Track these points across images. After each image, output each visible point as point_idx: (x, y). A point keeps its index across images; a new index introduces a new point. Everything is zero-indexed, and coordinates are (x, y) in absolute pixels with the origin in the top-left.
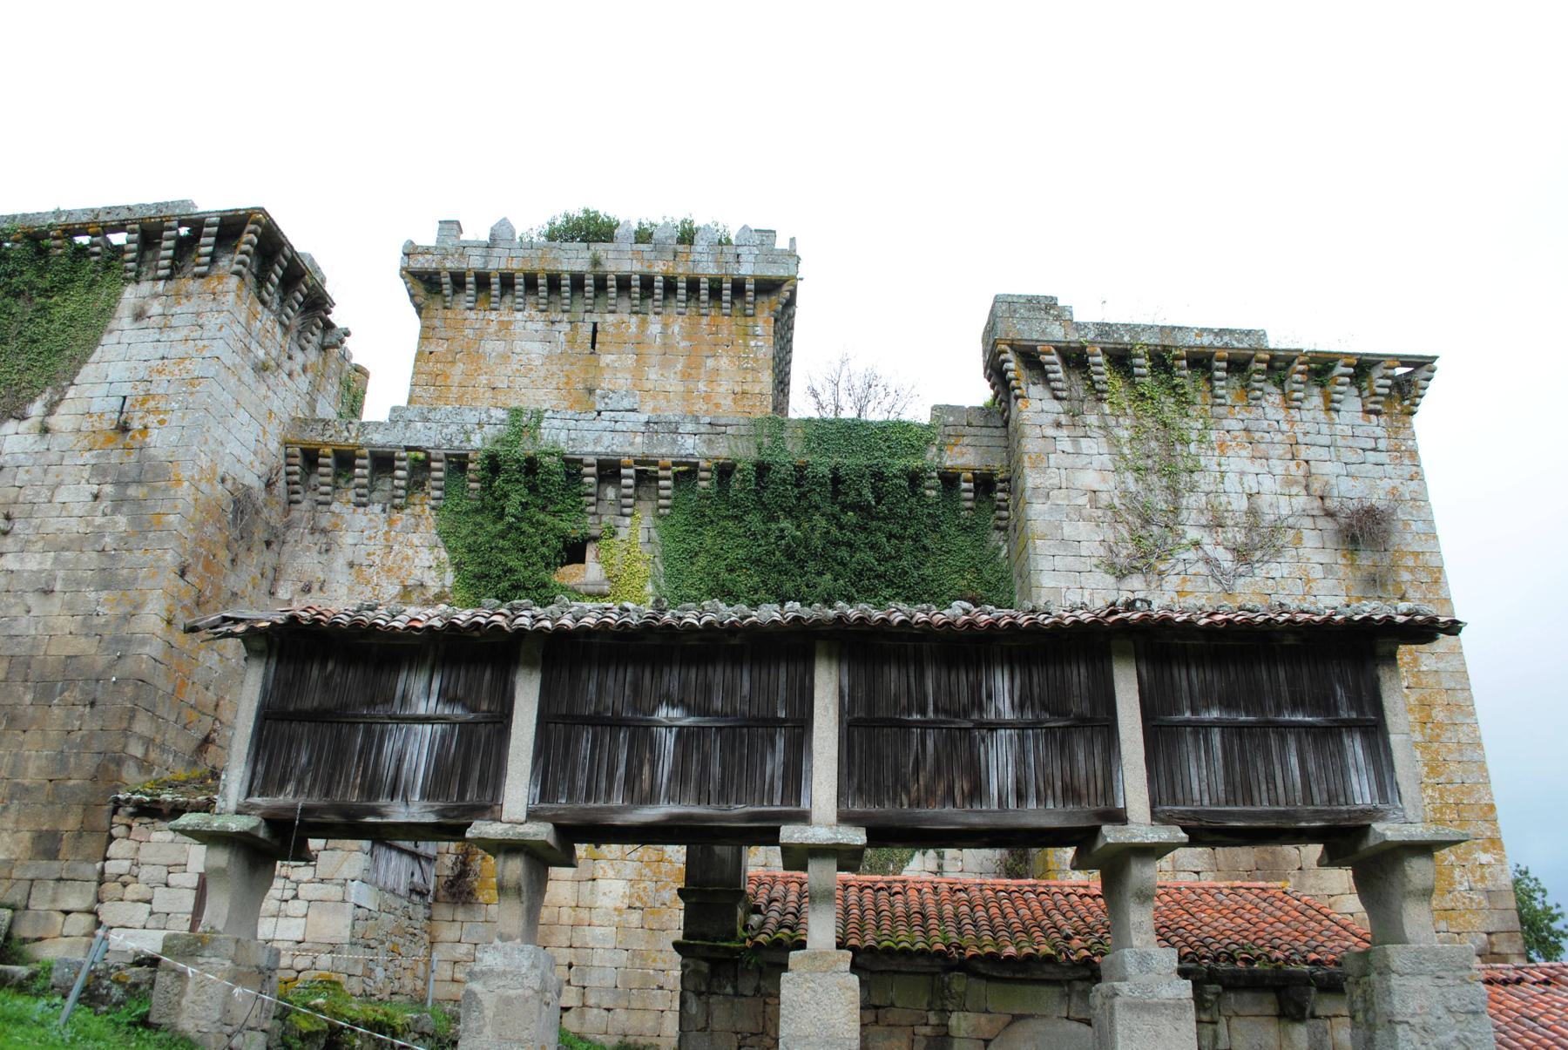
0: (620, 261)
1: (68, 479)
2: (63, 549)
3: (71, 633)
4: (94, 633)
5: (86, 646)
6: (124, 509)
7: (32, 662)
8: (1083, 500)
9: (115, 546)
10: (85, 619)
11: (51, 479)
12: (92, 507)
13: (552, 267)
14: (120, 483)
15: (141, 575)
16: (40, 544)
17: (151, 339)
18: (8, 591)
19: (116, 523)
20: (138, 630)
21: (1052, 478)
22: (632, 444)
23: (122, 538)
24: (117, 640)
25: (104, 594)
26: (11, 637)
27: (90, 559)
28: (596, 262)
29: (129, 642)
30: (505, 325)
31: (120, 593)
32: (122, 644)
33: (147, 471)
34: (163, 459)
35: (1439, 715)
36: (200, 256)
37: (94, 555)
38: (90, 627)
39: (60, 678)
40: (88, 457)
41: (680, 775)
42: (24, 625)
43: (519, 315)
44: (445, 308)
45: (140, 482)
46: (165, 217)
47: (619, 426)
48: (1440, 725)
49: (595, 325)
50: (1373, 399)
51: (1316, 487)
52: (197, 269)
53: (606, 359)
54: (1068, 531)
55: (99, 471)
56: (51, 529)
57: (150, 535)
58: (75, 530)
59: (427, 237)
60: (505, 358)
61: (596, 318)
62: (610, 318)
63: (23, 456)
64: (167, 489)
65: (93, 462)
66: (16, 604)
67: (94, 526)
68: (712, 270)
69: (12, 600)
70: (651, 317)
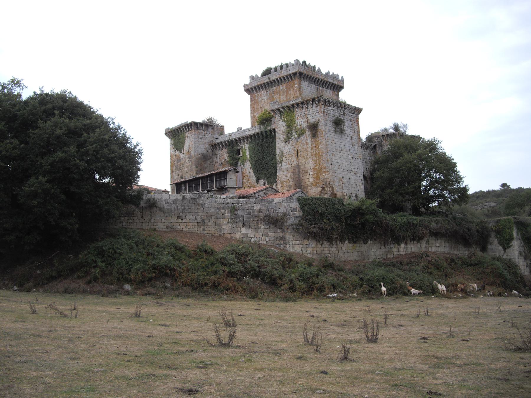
0: (274, 76)
13: (263, 82)
21: (279, 129)
28: (269, 79)
30: (261, 95)
35: (321, 154)
40: (187, 156)
41: (195, 189)
43: (262, 92)
48: (321, 156)
51: (309, 121)
53: (275, 96)
59: (248, 82)
60: (261, 101)
61: (272, 89)
62: (275, 88)
68: (286, 74)
70: (281, 86)
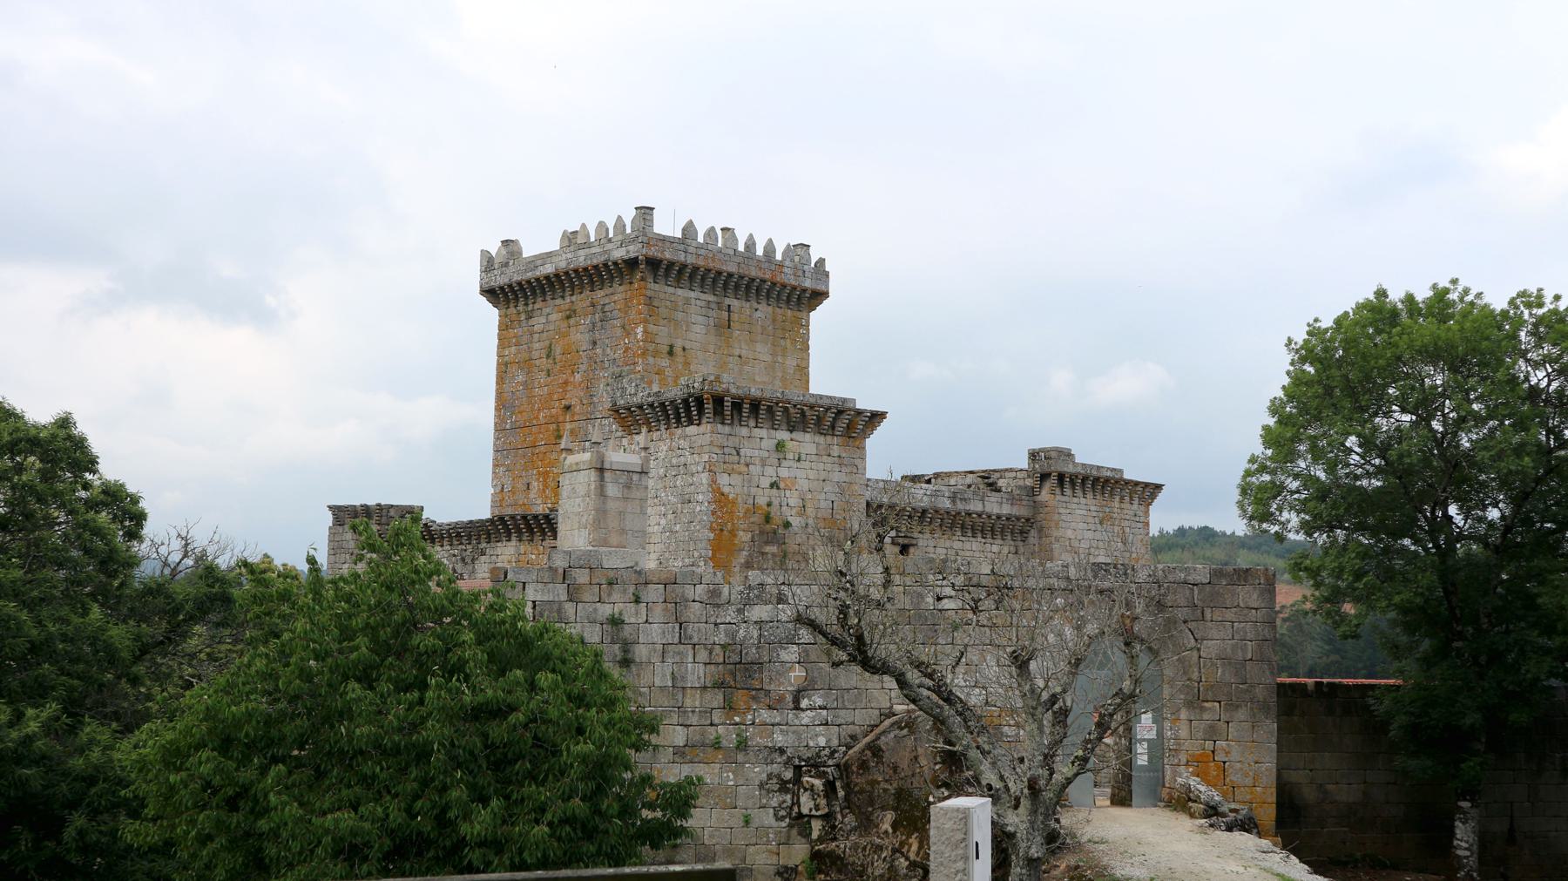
30: (687, 301)
49: (729, 306)
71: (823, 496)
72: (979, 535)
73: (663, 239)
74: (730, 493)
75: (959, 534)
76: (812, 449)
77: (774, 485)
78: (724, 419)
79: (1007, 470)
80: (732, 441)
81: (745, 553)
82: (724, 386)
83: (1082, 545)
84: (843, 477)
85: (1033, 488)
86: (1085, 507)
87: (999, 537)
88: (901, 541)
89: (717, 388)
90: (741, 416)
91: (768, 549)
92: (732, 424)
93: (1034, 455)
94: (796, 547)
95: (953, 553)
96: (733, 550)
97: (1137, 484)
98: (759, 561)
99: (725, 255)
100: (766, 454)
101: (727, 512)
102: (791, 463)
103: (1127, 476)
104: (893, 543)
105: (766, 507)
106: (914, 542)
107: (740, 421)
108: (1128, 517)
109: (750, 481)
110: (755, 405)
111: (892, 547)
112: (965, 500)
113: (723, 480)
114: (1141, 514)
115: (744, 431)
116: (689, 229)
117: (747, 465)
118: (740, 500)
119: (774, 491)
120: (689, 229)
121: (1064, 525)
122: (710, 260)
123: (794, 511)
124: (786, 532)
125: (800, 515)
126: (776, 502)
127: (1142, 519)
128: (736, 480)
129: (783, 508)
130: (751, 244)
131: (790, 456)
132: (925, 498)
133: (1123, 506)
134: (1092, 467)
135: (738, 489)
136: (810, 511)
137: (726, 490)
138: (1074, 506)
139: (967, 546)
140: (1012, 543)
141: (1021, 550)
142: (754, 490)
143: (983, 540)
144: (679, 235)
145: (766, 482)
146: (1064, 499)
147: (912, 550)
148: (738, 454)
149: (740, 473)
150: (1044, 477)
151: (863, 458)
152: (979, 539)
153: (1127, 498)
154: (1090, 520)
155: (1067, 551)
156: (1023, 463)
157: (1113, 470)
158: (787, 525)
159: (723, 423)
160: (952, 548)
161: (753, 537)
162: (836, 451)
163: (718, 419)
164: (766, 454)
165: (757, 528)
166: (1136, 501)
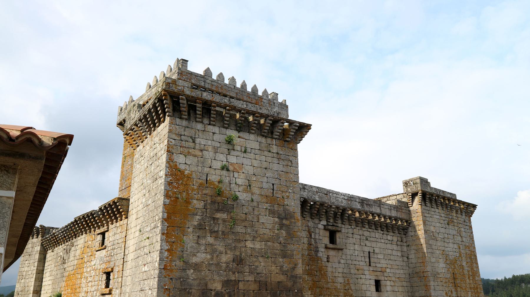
1: (262, 214)
2: (267, 241)
3: (277, 273)
4: (284, 273)
5: (282, 278)
6: (284, 228)
7: (267, 283)
8: (432, 234)
9: (284, 242)
10: (281, 268)
11: (256, 213)
12: (273, 226)
14: (281, 219)
15: (294, 253)
16: (258, 239)
17: (276, 163)
18: (251, 256)
19: (282, 233)
20: (298, 273)
22: (348, 204)
23: (285, 239)
24: (292, 276)
25: (284, 259)
26: (258, 274)
27: (277, 246)
29: (296, 277)
31: (289, 259)
32: (294, 278)
33: (287, 215)
34: (291, 211)
36: (289, 135)
37: (278, 244)
38: (283, 271)
39: (277, 290)
42: (259, 270)
44: (432, 207)
45: (286, 219)
46: (282, 118)
47: (346, 198)
50: (467, 213)
52: (287, 139)
54: (430, 242)
55: (272, 212)
56: (262, 233)
57: (294, 239)
58: (269, 234)
63: (244, 201)
64: (295, 223)
65: (269, 208)
66: (256, 261)
67: (275, 234)
69: (255, 259)
71: (265, 179)
72: (379, 229)
73: (191, 74)
74: (186, 170)
75: (367, 227)
76: (256, 145)
77: (223, 168)
78: (181, 115)
79: (391, 196)
80: (192, 133)
81: (198, 217)
82: (180, 88)
83: (440, 236)
84: (281, 168)
85: (407, 203)
86: (438, 214)
87: (391, 231)
88: (330, 227)
89: (174, 89)
90: (196, 114)
91: (218, 215)
92: (188, 119)
93: (406, 184)
94: (244, 216)
95: (365, 238)
96: (187, 214)
97: (464, 203)
98: (210, 226)
99: (228, 87)
100: (218, 145)
101: (182, 183)
102: (239, 153)
103: (458, 198)
104: (325, 229)
105: (217, 183)
106: (339, 229)
107: (196, 118)
108: (461, 223)
109: (203, 163)
110: (207, 107)
111: (325, 231)
112: (369, 205)
113: (180, 159)
114: (467, 222)
115: (200, 126)
116: (208, 72)
117: (201, 151)
118: (194, 175)
119: (224, 172)
120: (208, 72)
121: (428, 223)
122: (219, 89)
123: (241, 189)
124: (235, 204)
125: (245, 191)
126: (227, 180)
127: (468, 224)
128: (190, 160)
129: (233, 185)
130: (244, 85)
131: (238, 148)
132: (344, 201)
133: (458, 215)
134: (440, 191)
135: (194, 169)
136: (256, 190)
137: (182, 167)
138: (433, 213)
139: (373, 234)
140: (398, 235)
141: (405, 240)
142: (206, 170)
143: (382, 232)
144: (202, 73)
145: (218, 165)
146: (427, 208)
147: (338, 235)
148: (194, 142)
149: (195, 156)
150: (414, 195)
151: (296, 157)
152: (380, 231)
153: (459, 212)
154: (442, 222)
155: (432, 239)
156: (400, 189)
157: (451, 194)
158: (236, 198)
159: (181, 118)
160: (363, 235)
161: (205, 205)
162: (275, 149)
163: (177, 114)
164: (218, 145)
165: (209, 198)
166: (464, 214)
